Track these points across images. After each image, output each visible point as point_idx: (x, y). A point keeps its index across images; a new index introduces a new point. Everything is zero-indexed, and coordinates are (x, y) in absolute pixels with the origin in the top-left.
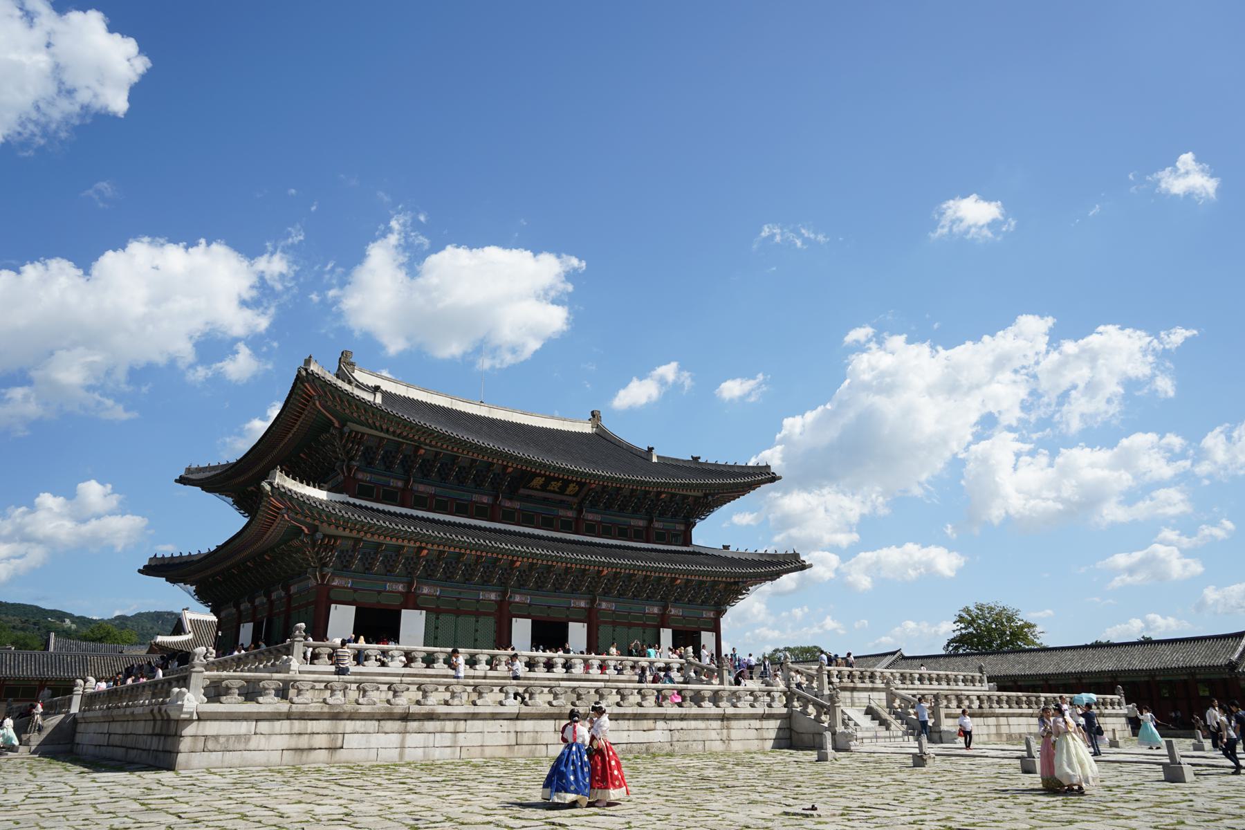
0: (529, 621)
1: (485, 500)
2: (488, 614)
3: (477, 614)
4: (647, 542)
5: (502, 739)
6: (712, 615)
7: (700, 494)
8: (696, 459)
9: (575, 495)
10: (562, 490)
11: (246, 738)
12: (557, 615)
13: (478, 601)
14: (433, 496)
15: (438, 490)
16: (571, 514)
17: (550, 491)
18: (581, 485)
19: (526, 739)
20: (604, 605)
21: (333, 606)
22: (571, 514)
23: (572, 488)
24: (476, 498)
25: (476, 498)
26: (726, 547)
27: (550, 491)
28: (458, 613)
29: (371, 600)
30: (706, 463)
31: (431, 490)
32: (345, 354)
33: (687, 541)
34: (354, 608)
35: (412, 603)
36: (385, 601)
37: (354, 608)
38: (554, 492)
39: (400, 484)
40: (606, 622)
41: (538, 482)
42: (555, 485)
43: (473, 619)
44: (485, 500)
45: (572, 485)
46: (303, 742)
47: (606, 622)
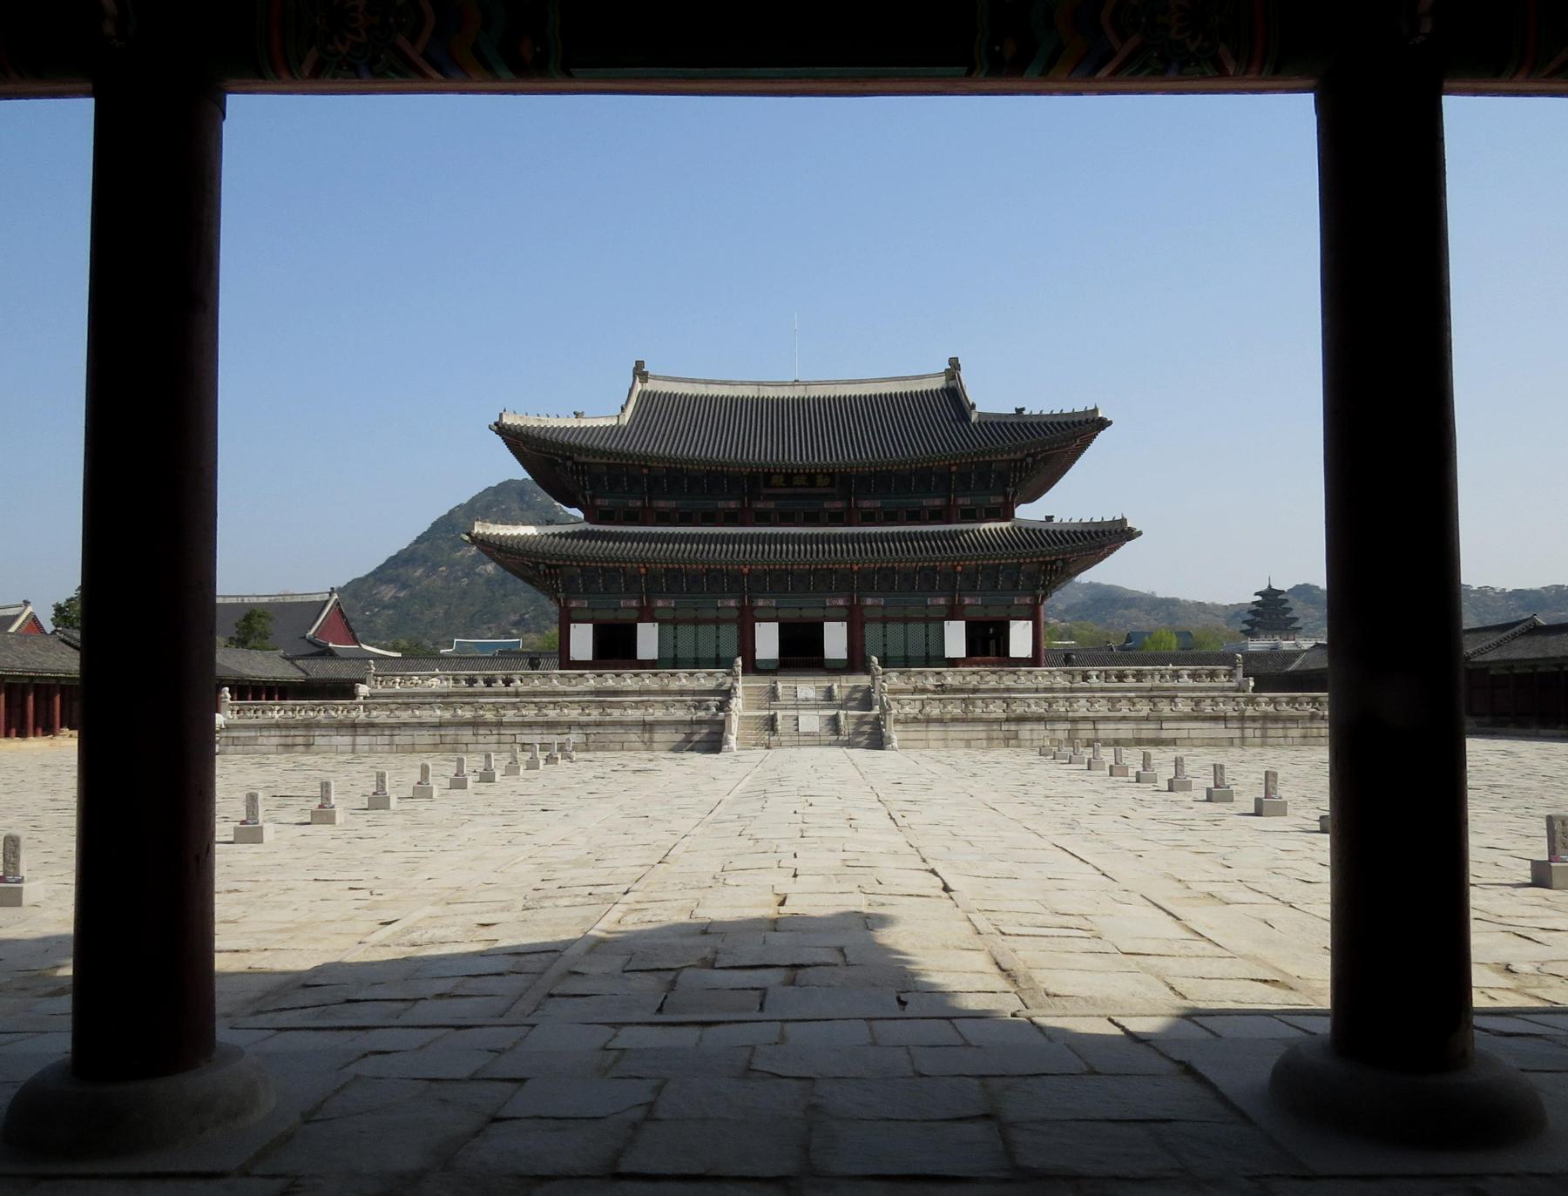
0: (776, 625)
1: (733, 504)
3: (717, 622)
4: (949, 522)
5: (429, 740)
6: (1028, 600)
7: (1019, 455)
8: (1019, 411)
9: (831, 485)
11: (256, 738)
12: (810, 614)
16: (839, 505)
18: (831, 475)
19: (448, 739)
20: (869, 601)
22: (839, 505)
24: (721, 504)
25: (721, 504)
26: (1049, 518)
29: (607, 616)
30: (1031, 416)
31: (673, 504)
32: (639, 365)
33: (1009, 516)
36: (622, 616)
39: (639, 503)
41: (775, 480)
43: (713, 627)
44: (733, 504)
45: (819, 479)
46: (289, 741)
47: (873, 620)
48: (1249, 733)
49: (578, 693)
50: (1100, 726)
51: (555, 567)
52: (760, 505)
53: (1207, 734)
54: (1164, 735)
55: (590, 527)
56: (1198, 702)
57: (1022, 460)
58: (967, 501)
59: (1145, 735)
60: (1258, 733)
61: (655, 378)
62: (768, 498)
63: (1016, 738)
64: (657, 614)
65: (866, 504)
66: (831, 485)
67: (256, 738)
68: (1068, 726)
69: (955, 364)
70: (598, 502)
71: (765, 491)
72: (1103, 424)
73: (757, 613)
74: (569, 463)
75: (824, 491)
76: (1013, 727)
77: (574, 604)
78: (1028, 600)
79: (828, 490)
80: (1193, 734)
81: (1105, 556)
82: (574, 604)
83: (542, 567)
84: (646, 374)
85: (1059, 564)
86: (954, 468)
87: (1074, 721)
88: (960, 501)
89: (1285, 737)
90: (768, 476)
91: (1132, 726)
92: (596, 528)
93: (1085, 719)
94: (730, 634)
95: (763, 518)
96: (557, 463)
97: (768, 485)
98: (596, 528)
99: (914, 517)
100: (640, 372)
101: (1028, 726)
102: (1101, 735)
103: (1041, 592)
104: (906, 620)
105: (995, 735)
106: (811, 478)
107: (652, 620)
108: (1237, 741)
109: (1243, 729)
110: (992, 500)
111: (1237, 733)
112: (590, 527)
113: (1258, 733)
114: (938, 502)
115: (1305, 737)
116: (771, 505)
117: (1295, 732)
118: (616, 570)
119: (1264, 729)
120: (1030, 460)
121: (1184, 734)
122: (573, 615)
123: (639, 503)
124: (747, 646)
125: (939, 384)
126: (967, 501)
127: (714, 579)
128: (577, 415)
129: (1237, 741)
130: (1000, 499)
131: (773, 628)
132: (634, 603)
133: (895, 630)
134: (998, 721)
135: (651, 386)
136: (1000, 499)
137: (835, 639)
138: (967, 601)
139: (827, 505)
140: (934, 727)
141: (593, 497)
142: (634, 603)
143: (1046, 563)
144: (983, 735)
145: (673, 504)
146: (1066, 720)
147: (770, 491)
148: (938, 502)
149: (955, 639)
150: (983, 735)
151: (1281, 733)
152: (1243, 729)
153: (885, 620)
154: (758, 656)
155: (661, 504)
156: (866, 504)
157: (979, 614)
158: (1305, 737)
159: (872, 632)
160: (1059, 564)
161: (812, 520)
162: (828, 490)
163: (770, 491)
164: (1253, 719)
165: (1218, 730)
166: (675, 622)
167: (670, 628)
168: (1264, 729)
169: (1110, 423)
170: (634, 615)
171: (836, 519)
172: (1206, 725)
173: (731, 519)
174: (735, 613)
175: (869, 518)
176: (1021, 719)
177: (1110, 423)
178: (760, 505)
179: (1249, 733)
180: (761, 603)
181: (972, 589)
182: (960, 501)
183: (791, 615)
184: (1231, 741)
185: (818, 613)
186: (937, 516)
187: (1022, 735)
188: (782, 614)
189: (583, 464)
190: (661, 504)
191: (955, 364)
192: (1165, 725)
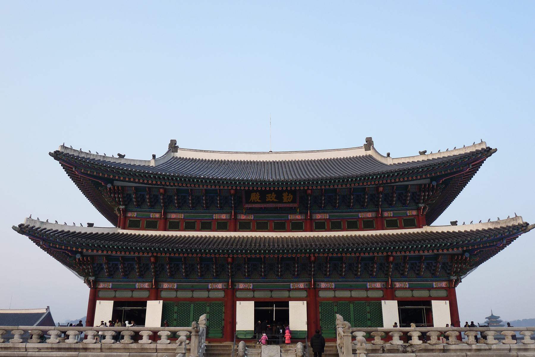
0: (252, 303)
1: (224, 216)
10: (280, 199)
16: (298, 217)
17: (269, 202)
18: (293, 192)
21: (98, 302)
22: (298, 217)
23: (286, 197)
24: (216, 216)
25: (216, 216)
26: (454, 223)
29: (126, 295)
31: (181, 216)
36: (137, 295)
37: (113, 301)
39: (158, 215)
41: (255, 197)
42: (271, 197)
44: (224, 216)
45: (285, 195)
49: (39, 350)
51: (87, 256)
52: (243, 217)
55: (121, 231)
57: (429, 185)
58: (391, 214)
62: (251, 211)
64: (164, 294)
65: (318, 216)
66: (292, 202)
70: (129, 215)
71: (246, 206)
72: (488, 152)
73: (238, 294)
74: (109, 186)
75: (288, 205)
78: (444, 284)
79: (291, 205)
81: (502, 248)
82: (101, 285)
83: (78, 256)
84: (177, 147)
85: (467, 255)
86: (381, 189)
88: (386, 214)
90: (248, 193)
92: (125, 232)
95: (245, 227)
96: (102, 186)
97: (248, 202)
98: (125, 232)
99: (352, 226)
100: (173, 146)
103: (454, 278)
106: (279, 195)
107: (157, 298)
110: (409, 213)
112: (121, 231)
114: (370, 215)
116: (251, 217)
118: (133, 259)
120: (434, 183)
122: (101, 294)
123: (158, 215)
125: (362, 153)
126: (391, 214)
128: (121, 156)
130: (414, 213)
132: (146, 285)
135: (179, 154)
136: (414, 213)
137: (298, 316)
139: (291, 217)
141: (125, 211)
142: (146, 285)
143: (458, 255)
145: (181, 216)
147: (250, 206)
148: (370, 215)
154: (239, 328)
155: (173, 216)
156: (318, 216)
160: (467, 255)
162: (291, 205)
163: (250, 206)
169: (496, 150)
170: (146, 294)
173: (222, 227)
174: (221, 294)
175: (320, 227)
177: (496, 150)
178: (243, 217)
181: (403, 277)
182: (386, 214)
185: (285, 294)
186: (368, 225)
188: (259, 295)
189: (118, 187)
190: (173, 216)
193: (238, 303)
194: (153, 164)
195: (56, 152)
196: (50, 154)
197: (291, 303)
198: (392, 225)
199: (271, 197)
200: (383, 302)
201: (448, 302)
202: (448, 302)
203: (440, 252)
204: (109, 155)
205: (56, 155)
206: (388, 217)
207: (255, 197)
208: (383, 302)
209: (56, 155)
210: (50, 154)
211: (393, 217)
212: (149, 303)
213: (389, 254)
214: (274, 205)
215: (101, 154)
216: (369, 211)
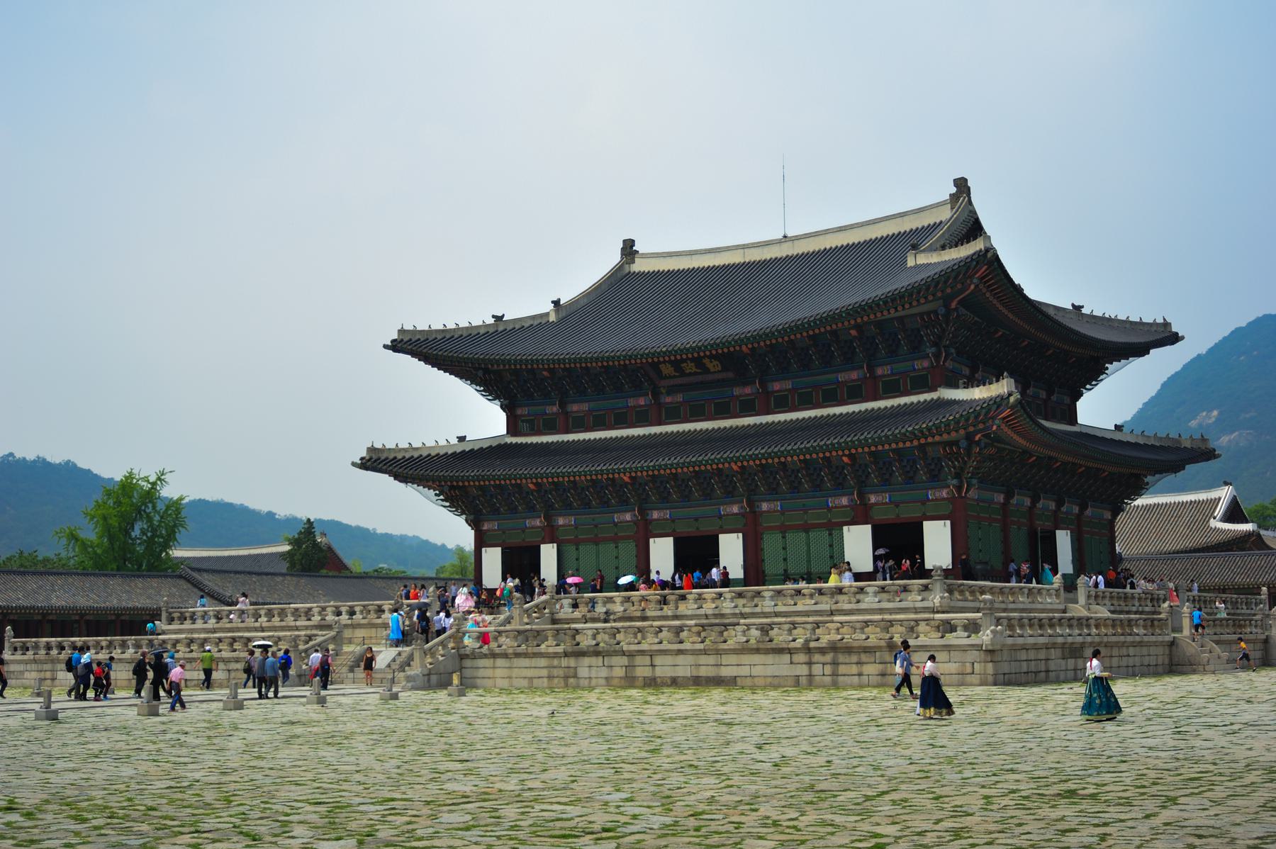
0: (671, 540)
2: (628, 538)
3: (615, 540)
9: (725, 369)
12: (706, 528)
13: (615, 524)
14: (590, 411)
15: (592, 405)
25: (631, 402)
27: (690, 374)
28: (596, 541)
29: (516, 540)
34: (499, 549)
35: (551, 536)
38: (696, 373)
40: (771, 528)
43: (612, 545)
44: (642, 401)
47: (771, 528)
48: (817, 669)
50: (658, 660)
53: (770, 671)
54: (726, 672)
56: (765, 629)
59: (704, 672)
60: (828, 670)
61: (645, 256)
63: (575, 676)
66: (725, 369)
67: (22, 672)
68: (624, 660)
69: (962, 185)
75: (717, 376)
76: (572, 662)
77: (485, 528)
80: (757, 671)
85: (963, 444)
87: (631, 655)
88: (879, 371)
89: (860, 675)
91: (689, 659)
93: (642, 653)
94: (628, 550)
100: (629, 249)
101: (587, 661)
102: (659, 672)
104: (806, 528)
105: (555, 672)
108: (803, 680)
109: (810, 664)
111: (803, 670)
113: (828, 670)
115: (883, 675)
117: (871, 669)
119: (835, 663)
121: (744, 671)
123: (555, 409)
124: (643, 569)
127: (604, 494)
128: (499, 319)
129: (803, 680)
131: (669, 541)
133: (796, 540)
134: (556, 655)
135: (639, 266)
136: (926, 364)
138: (873, 499)
139: (737, 391)
140: (500, 662)
144: (545, 672)
146: (623, 653)
149: (858, 544)
150: (545, 672)
151: (854, 669)
152: (810, 664)
153: (784, 530)
157: (888, 516)
158: (883, 675)
159: (771, 544)
161: (723, 411)
164: (822, 651)
165: (780, 666)
166: (577, 543)
167: (570, 550)
168: (835, 663)
171: (748, 408)
172: (770, 659)
176: (582, 654)
179: (817, 669)
180: (655, 515)
183: (686, 529)
184: (811, 683)
187: (583, 672)
191: (962, 185)
192: (726, 659)
193: (651, 540)
194: (552, 318)
195: (393, 341)
196: (386, 347)
197: (721, 536)
198: (893, 389)
199: (690, 367)
200: (845, 528)
201: (948, 522)
202: (948, 522)
203: (930, 440)
204: (477, 322)
205: (395, 346)
206: (884, 376)
207: (667, 370)
208: (845, 528)
209: (395, 346)
210: (386, 347)
211: (892, 374)
212: (543, 547)
213: (840, 453)
214: (700, 378)
215: (464, 324)
216: (854, 369)
